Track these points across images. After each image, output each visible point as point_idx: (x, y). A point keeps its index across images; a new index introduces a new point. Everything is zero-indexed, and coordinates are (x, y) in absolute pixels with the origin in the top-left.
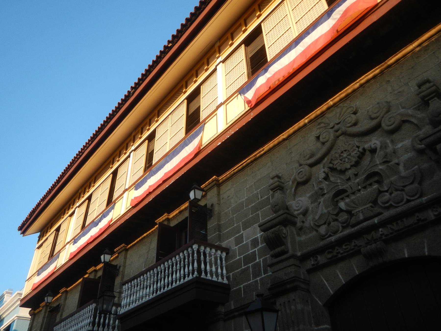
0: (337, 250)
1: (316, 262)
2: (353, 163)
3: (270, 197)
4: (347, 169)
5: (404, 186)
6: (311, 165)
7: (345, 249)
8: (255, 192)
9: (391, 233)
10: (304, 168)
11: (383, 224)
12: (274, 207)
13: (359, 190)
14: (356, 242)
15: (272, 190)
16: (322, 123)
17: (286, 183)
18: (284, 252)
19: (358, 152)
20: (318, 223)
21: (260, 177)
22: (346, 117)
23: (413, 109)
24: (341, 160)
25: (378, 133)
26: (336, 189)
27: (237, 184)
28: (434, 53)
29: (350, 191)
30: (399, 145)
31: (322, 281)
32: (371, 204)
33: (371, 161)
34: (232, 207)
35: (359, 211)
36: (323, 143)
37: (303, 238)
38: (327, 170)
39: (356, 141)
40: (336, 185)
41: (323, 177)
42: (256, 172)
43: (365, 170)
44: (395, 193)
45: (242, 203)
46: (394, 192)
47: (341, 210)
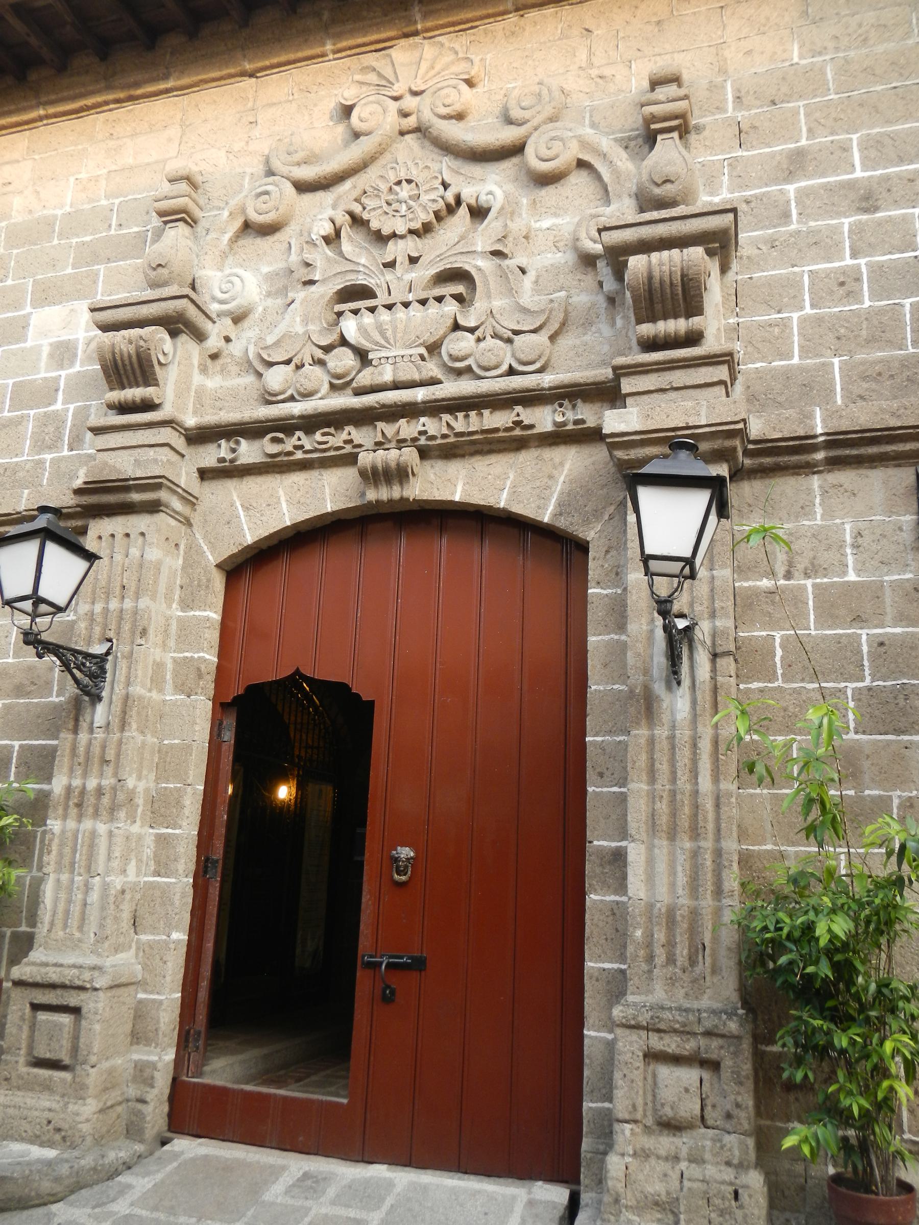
0: (299, 439)
1: (233, 456)
2: (417, 225)
3: (150, 234)
4: (394, 235)
5: (517, 333)
6: (303, 187)
7: (320, 443)
8: (104, 202)
9: (444, 436)
10: (277, 186)
11: (434, 408)
12: (154, 269)
13: (406, 305)
15: (161, 214)
16: (374, 70)
17: (211, 210)
18: (148, 406)
19: (440, 200)
20: (269, 355)
21: (131, 161)
23: (616, 140)
24: (389, 204)
25: (508, 166)
26: (347, 278)
28: (722, 7)
29: (382, 298)
30: (546, 223)
31: (232, 505)
33: (462, 238)
34: (13, 221)
36: (357, 135)
37: (213, 383)
38: (340, 216)
39: (446, 166)
40: (351, 267)
41: (323, 233)
42: (125, 140)
43: (441, 255)
44: (490, 342)
45: (49, 222)
46: (488, 338)
47: (343, 342)
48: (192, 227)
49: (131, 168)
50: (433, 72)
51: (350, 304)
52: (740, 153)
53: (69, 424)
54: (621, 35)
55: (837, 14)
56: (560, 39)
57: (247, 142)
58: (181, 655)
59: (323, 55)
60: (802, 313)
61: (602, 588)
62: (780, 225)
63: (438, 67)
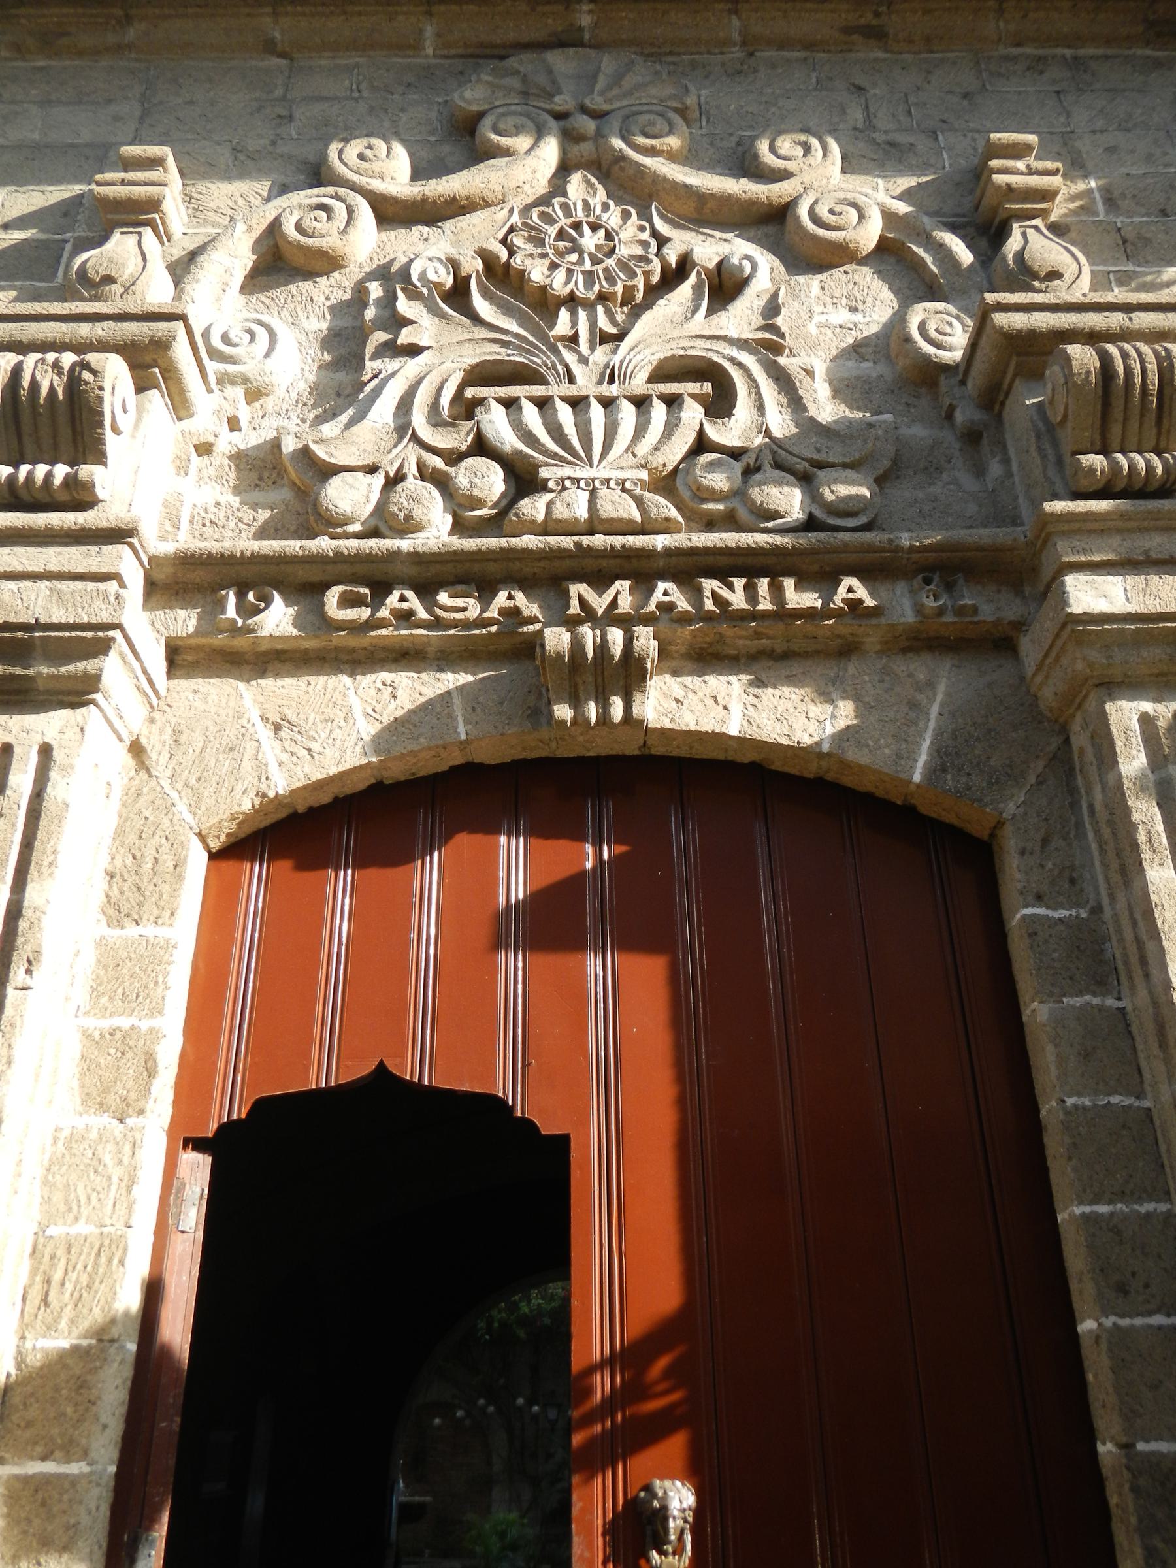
0: (403, 599)
4: (572, 301)
5: (821, 465)
14: (519, 595)
21: (36, 136)
22: (646, 108)
28: (1058, 93)
35: (576, 481)
47: (482, 447)
48: (162, 244)
49: (36, 147)
50: (615, 91)
51: (497, 389)
52: (1130, 267)
54: (912, 99)
56: (815, 89)
57: (273, 143)
61: (1048, 908)
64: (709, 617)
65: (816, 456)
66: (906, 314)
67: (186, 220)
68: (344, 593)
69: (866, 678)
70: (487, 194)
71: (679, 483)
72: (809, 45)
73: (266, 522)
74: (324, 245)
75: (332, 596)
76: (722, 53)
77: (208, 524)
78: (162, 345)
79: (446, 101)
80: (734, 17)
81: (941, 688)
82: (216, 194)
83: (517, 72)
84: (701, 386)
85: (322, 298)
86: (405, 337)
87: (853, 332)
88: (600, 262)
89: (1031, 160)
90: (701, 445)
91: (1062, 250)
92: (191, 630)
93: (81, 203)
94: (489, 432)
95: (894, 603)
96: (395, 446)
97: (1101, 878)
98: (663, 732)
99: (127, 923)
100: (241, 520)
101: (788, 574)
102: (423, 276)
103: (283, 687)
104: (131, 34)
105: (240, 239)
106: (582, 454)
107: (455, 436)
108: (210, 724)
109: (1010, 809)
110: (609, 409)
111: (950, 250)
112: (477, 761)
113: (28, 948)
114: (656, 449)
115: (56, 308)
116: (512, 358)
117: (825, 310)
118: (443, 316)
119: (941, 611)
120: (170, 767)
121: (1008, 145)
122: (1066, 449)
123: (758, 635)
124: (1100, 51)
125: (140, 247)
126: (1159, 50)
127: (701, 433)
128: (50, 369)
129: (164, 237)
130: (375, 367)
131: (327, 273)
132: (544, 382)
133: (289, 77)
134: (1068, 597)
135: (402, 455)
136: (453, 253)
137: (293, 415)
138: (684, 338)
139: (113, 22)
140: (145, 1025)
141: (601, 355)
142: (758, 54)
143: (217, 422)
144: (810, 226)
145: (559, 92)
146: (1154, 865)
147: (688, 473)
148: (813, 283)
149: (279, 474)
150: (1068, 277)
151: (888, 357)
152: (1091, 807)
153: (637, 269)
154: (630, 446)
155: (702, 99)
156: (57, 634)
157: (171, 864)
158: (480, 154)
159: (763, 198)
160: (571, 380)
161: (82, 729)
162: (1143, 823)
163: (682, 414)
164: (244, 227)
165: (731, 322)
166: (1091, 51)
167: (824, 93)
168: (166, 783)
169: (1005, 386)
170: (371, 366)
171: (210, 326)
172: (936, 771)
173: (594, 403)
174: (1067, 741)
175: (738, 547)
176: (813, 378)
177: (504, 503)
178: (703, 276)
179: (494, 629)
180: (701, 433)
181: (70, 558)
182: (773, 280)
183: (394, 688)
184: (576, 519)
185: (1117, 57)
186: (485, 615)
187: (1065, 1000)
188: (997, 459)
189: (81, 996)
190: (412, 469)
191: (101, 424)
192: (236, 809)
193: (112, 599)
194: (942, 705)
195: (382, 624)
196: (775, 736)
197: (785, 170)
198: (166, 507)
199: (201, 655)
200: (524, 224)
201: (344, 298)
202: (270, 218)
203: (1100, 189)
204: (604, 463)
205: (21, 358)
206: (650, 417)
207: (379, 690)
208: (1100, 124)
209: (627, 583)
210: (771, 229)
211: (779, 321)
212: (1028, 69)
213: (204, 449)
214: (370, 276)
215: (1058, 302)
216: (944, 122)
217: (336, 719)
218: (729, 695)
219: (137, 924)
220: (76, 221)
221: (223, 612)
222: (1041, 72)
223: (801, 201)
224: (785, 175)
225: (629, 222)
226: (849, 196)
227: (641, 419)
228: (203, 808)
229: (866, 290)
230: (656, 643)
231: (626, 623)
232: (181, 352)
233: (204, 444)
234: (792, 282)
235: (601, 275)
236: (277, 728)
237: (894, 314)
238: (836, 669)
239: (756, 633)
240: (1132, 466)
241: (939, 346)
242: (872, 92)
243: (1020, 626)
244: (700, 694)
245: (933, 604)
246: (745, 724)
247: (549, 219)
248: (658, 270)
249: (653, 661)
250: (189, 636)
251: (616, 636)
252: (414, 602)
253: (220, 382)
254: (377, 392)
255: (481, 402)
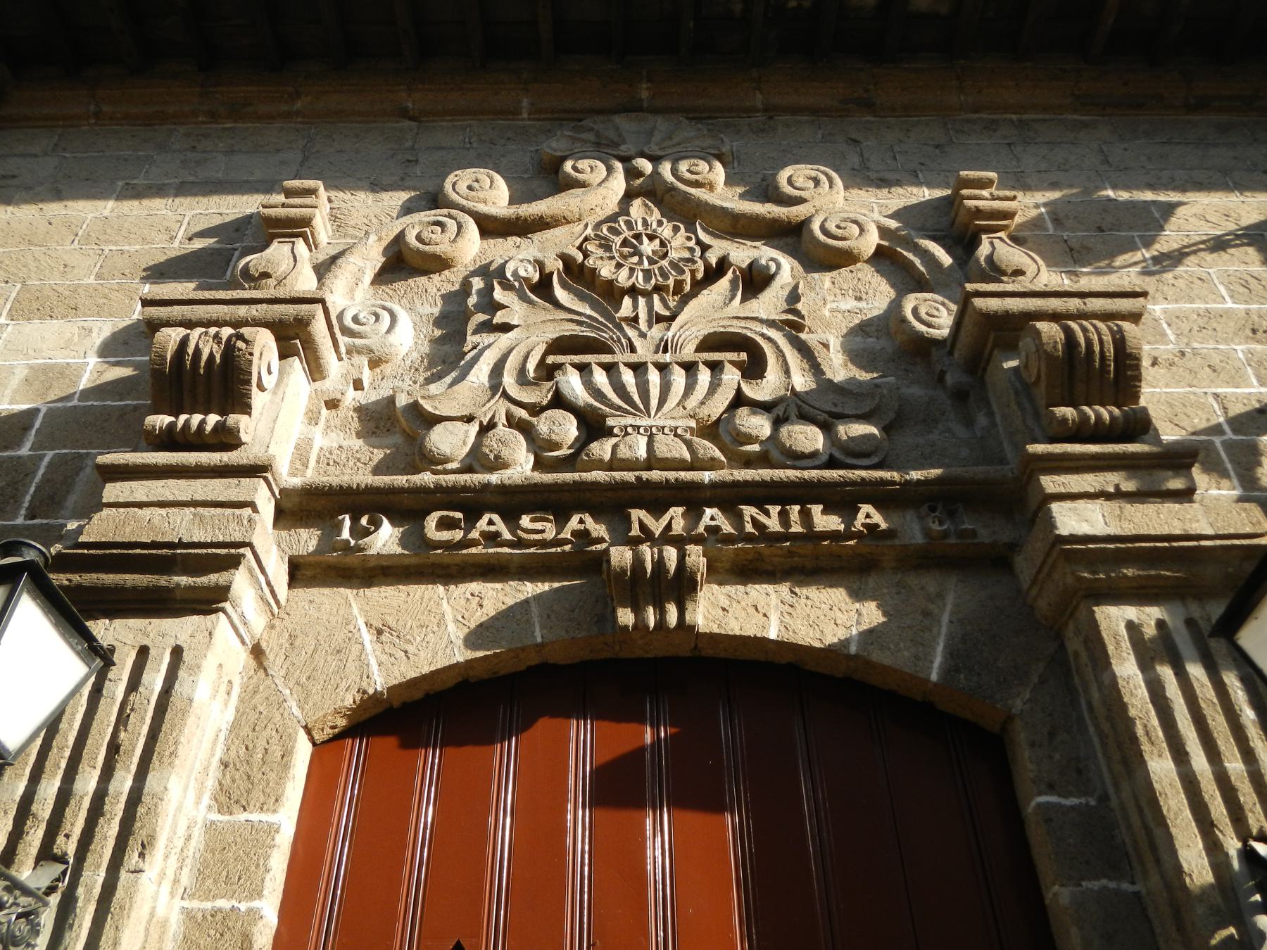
0: (491, 522)
4: (633, 291)
10: (455, 219)
21: (220, 175)
22: (690, 154)
27: (85, 152)
28: (1009, 145)
32: (693, 424)
35: (636, 428)
42: (214, 154)
47: (559, 401)
48: (311, 250)
51: (572, 357)
53: (37, 479)
54: (896, 148)
55: (1142, 167)
56: (821, 142)
58: (208, 905)
59: (514, 113)
60: (1225, 438)
61: (1060, 795)
62: (1156, 342)
63: (676, 140)
64: (749, 538)
65: (833, 409)
66: (901, 301)
67: (331, 233)
68: (442, 518)
69: (885, 591)
70: (567, 214)
71: (721, 430)
72: (815, 111)
73: (380, 462)
74: (438, 250)
75: (432, 521)
76: (749, 117)
77: (331, 463)
78: (302, 324)
79: (537, 150)
80: (757, 92)
81: (950, 599)
82: (355, 215)
83: (592, 129)
84: (738, 355)
85: (435, 290)
86: (499, 318)
87: (859, 315)
88: (656, 262)
89: (993, 190)
90: (739, 400)
91: (1023, 254)
92: (311, 549)
93: (250, 222)
94: (566, 391)
95: (906, 527)
96: (489, 401)
97: (1104, 769)
98: (712, 637)
99: (236, 808)
100: (359, 460)
101: (816, 502)
102: (515, 273)
103: (386, 597)
104: (298, 105)
105: (372, 246)
106: (642, 407)
107: (538, 393)
108: (321, 629)
109: (1018, 705)
110: (664, 372)
111: (933, 255)
112: (551, 661)
113: (143, 832)
114: (702, 403)
115: (221, 295)
116: (585, 334)
117: (836, 299)
118: (530, 302)
119: (945, 534)
120: (285, 667)
121: (974, 179)
122: (1042, 403)
123: (790, 553)
124: (1040, 116)
125: (293, 252)
126: (1084, 115)
127: (739, 390)
128: (211, 340)
129: (312, 245)
130: (474, 340)
131: (439, 271)
132: (610, 351)
133: (417, 134)
134: (1055, 521)
135: (494, 408)
136: (540, 256)
137: (407, 378)
138: (724, 318)
139: (286, 96)
140: (243, 907)
141: (656, 331)
142: (776, 118)
143: (344, 383)
144: (822, 237)
145: (624, 142)
146: (1154, 757)
147: (728, 423)
148: (826, 279)
149: (392, 423)
150: (1030, 274)
151: (888, 334)
152: (1089, 704)
153: (685, 268)
154: (681, 401)
155: (734, 149)
156: (196, 551)
157: (279, 754)
158: (561, 184)
159: (784, 217)
160: (633, 350)
161: (210, 633)
162: (1140, 718)
163: (723, 376)
164: (376, 238)
165: (761, 307)
166: (1033, 116)
167: (828, 144)
168: (279, 681)
169: (986, 356)
170: (471, 339)
171: (344, 310)
172: (950, 671)
173: (651, 367)
174: (1062, 646)
175: (773, 481)
176: (828, 350)
177: (578, 445)
178: (738, 273)
179: (567, 548)
180: (739, 390)
181: (214, 490)
182: (793, 277)
183: (481, 598)
184: (637, 458)
185: (1052, 120)
186: (559, 537)
187: (1084, 883)
188: (982, 413)
189: (186, 879)
190: (501, 419)
191: (248, 382)
192: (339, 704)
193: (245, 522)
194: (952, 614)
195: (474, 543)
196: (809, 640)
197: (800, 197)
198: (298, 450)
199: (318, 571)
200: (596, 235)
201: (452, 290)
202: (400, 229)
203: (1048, 213)
204: (659, 414)
205: (189, 331)
206: (697, 379)
207: (468, 600)
208: (1043, 166)
209: (680, 510)
210: (790, 240)
211: (799, 306)
212: (985, 128)
213: (332, 404)
214: (474, 273)
215: (1025, 290)
216: (922, 164)
217: (431, 625)
218: (768, 605)
219: (245, 809)
220: (244, 235)
221: (339, 534)
222: (995, 131)
223: (813, 219)
224: (800, 201)
225: (679, 234)
226: (851, 216)
227: (690, 381)
228: (311, 703)
229: (867, 285)
230: (705, 559)
231: (679, 542)
232: (319, 328)
233: (333, 400)
234: (809, 278)
235: (657, 272)
236: (380, 632)
237: (891, 302)
238: (858, 583)
239: (789, 552)
240: (1098, 416)
241: (929, 325)
242: (865, 144)
243: (1013, 547)
244: (743, 604)
245: (939, 528)
246: (783, 629)
247: (617, 232)
248: (702, 269)
249: (703, 575)
250: (309, 555)
251: (671, 554)
252: (500, 526)
253: (349, 352)
254: (476, 359)
255: (559, 366)
